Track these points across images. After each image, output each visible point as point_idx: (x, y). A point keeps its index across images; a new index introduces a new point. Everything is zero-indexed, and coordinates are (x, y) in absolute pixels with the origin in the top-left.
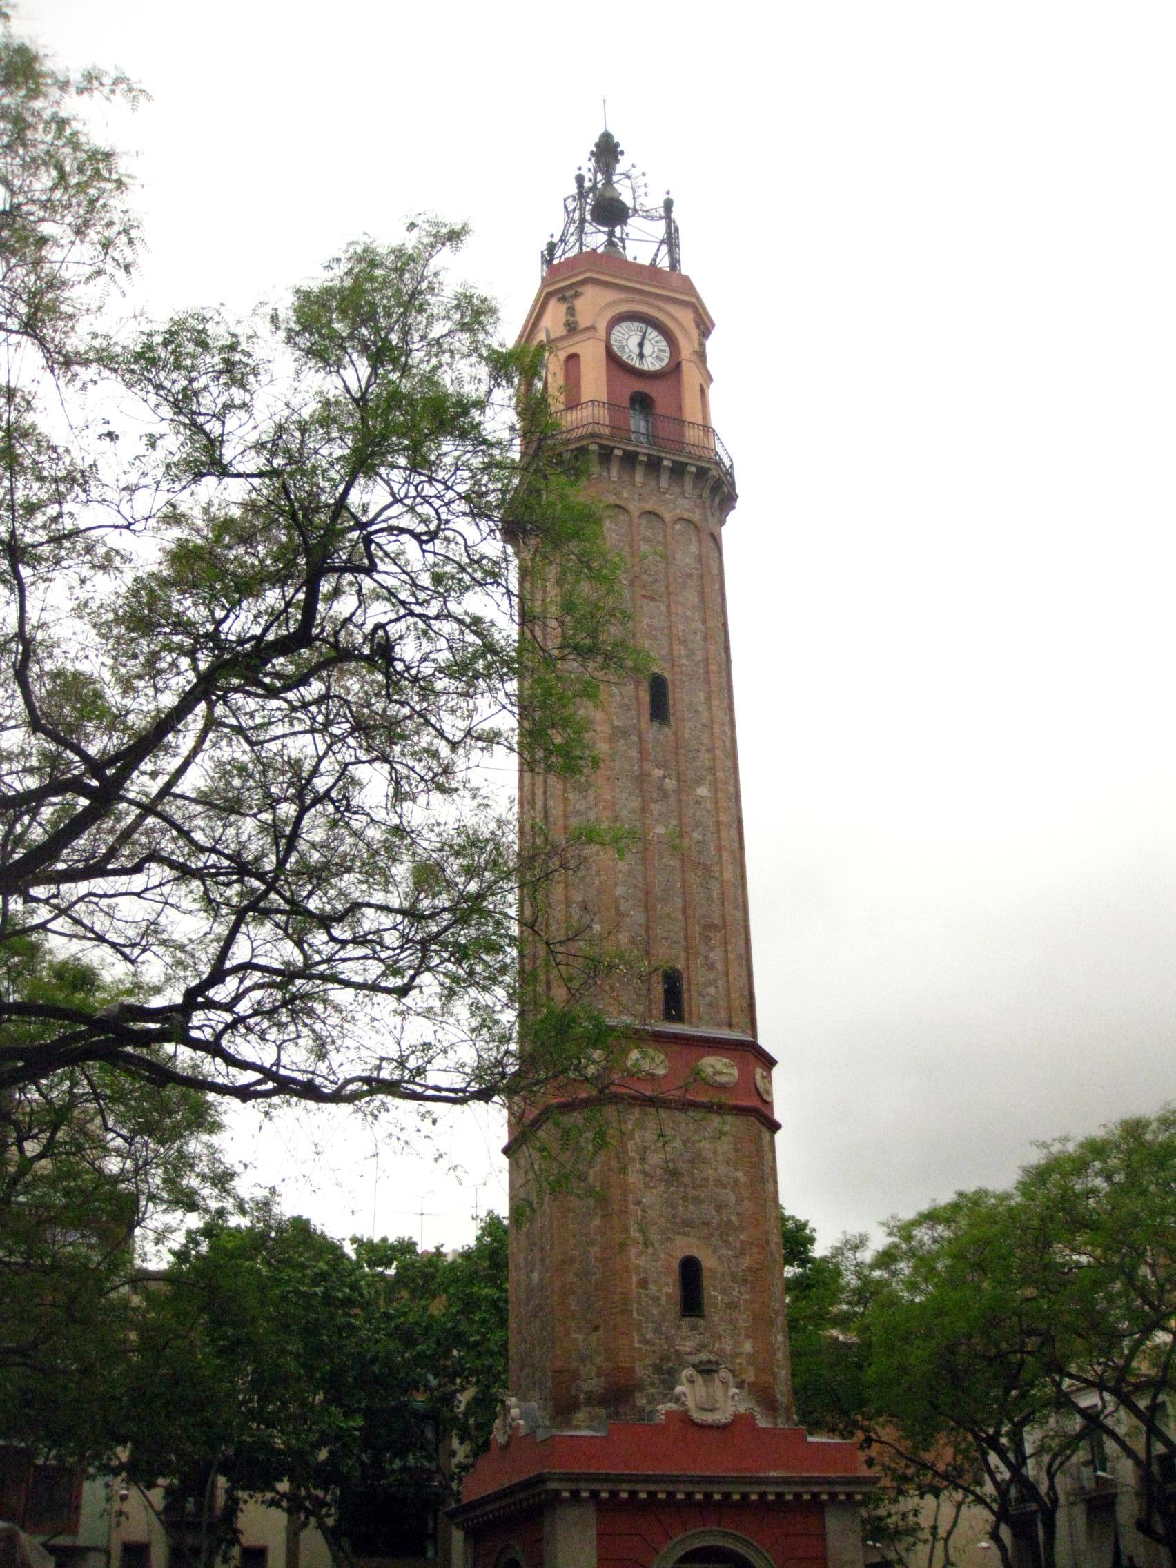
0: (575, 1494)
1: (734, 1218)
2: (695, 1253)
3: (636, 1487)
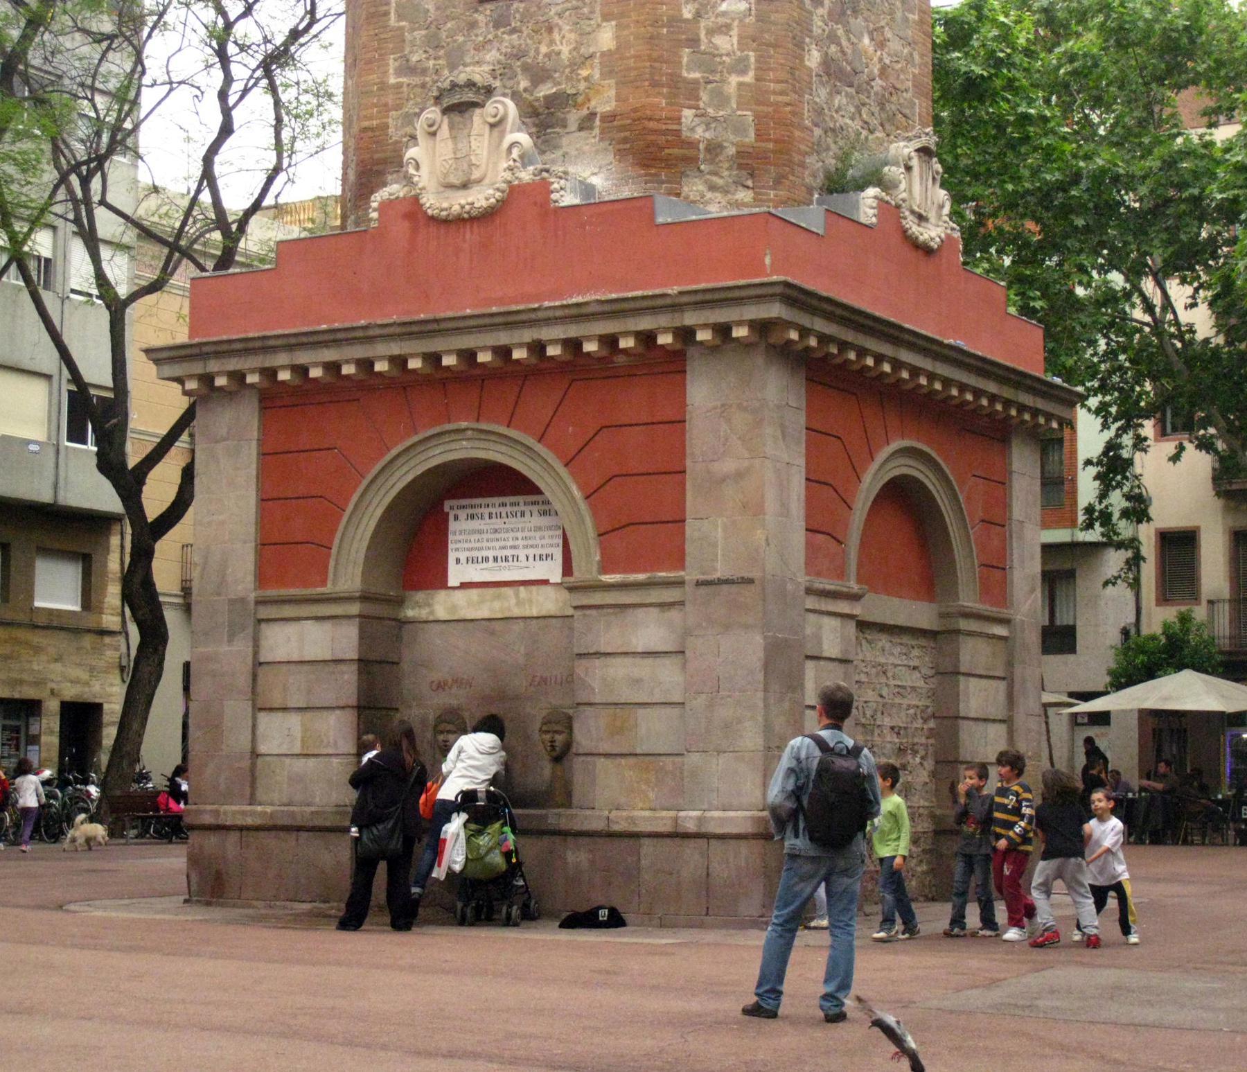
3: (302, 358)
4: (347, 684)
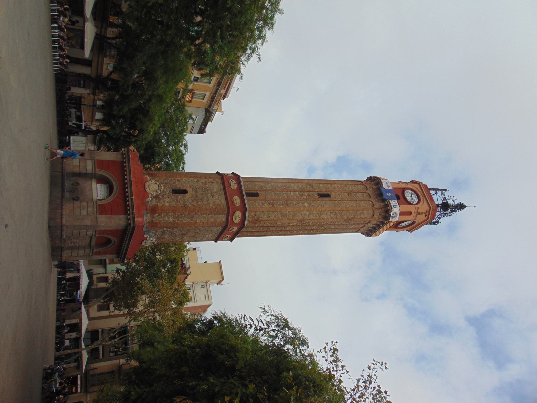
1: (200, 203)
2: (189, 193)
4: (84, 171)
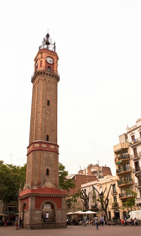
0: (33, 196)
1: (53, 164)
2: (48, 168)
